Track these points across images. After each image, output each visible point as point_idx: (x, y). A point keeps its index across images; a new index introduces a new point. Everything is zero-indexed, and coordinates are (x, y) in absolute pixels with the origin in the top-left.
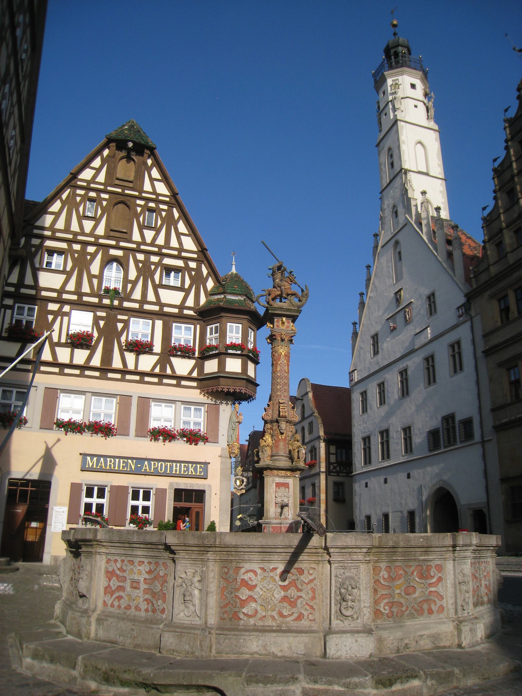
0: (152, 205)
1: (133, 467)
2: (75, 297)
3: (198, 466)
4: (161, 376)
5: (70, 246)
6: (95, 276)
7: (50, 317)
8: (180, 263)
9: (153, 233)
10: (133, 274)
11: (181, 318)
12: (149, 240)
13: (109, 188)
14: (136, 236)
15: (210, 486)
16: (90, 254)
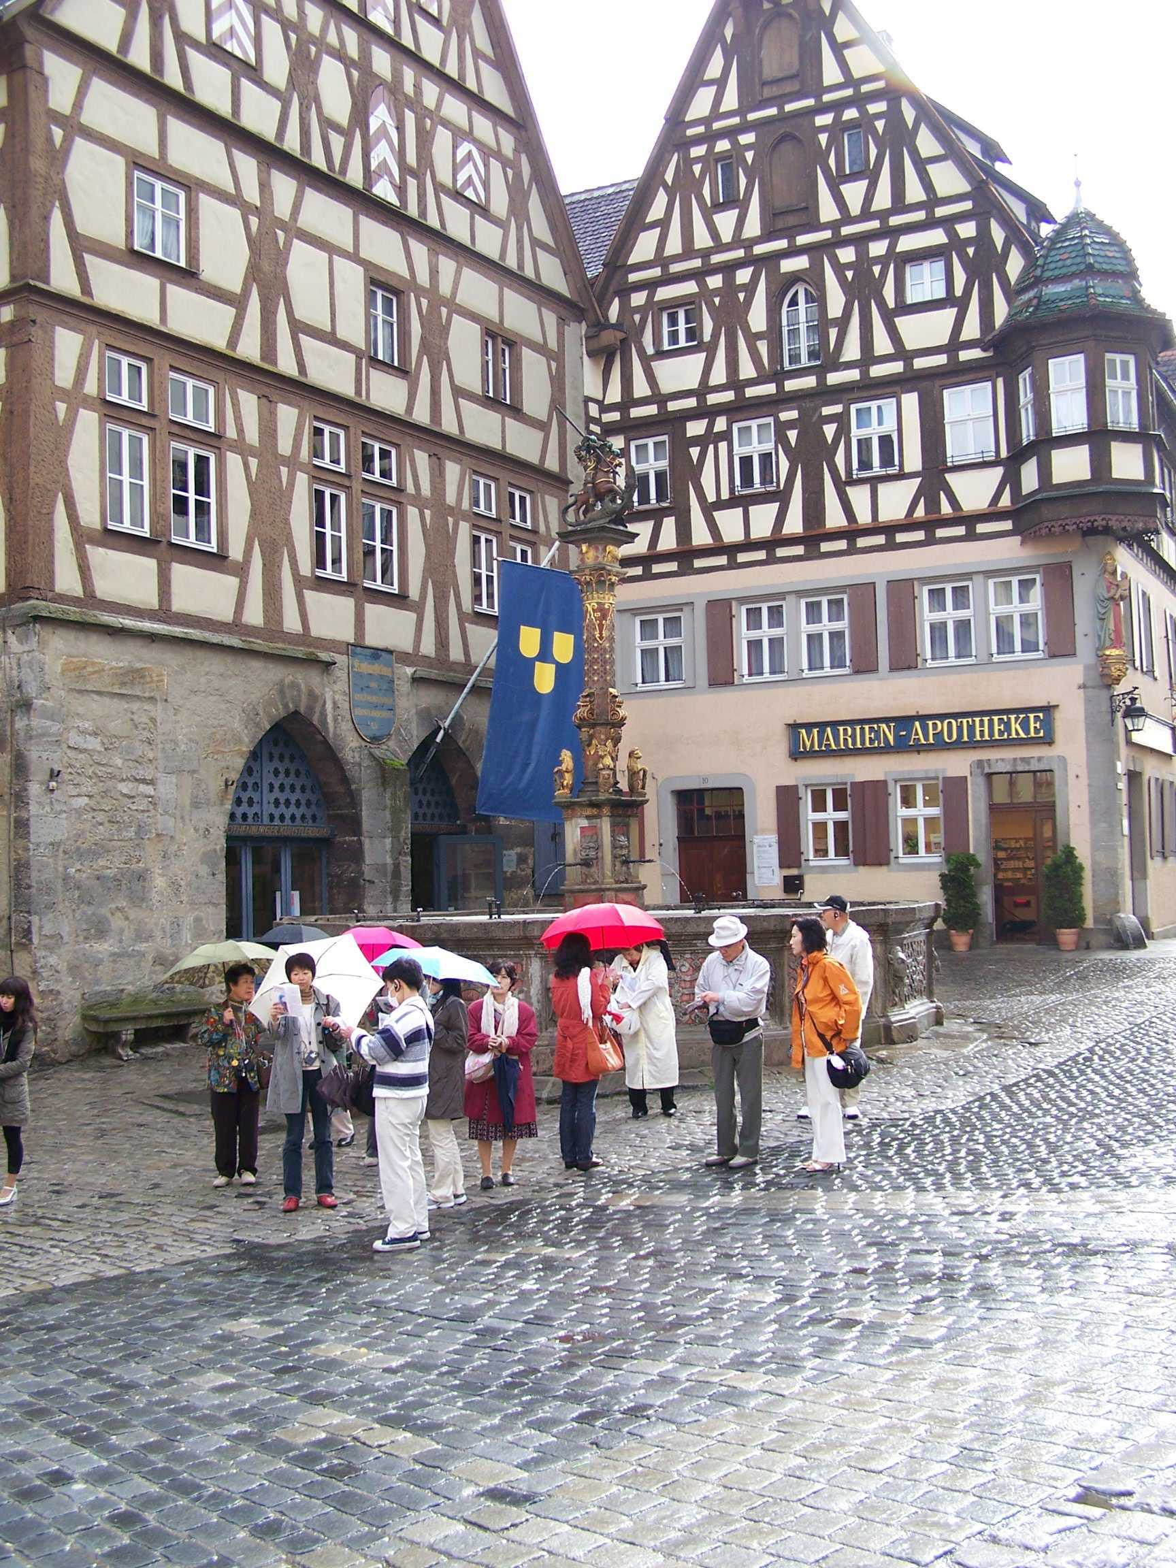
0: (851, 114)
1: (891, 738)
2: (729, 396)
3: (1032, 716)
4: (929, 525)
5: (702, 285)
6: (760, 336)
7: (695, 452)
8: (937, 237)
9: (863, 184)
10: (836, 302)
11: (958, 374)
12: (855, 209)
13: (752, 117)
14: (828, 211)
15: (1063, 760)
16: (744, 287)
